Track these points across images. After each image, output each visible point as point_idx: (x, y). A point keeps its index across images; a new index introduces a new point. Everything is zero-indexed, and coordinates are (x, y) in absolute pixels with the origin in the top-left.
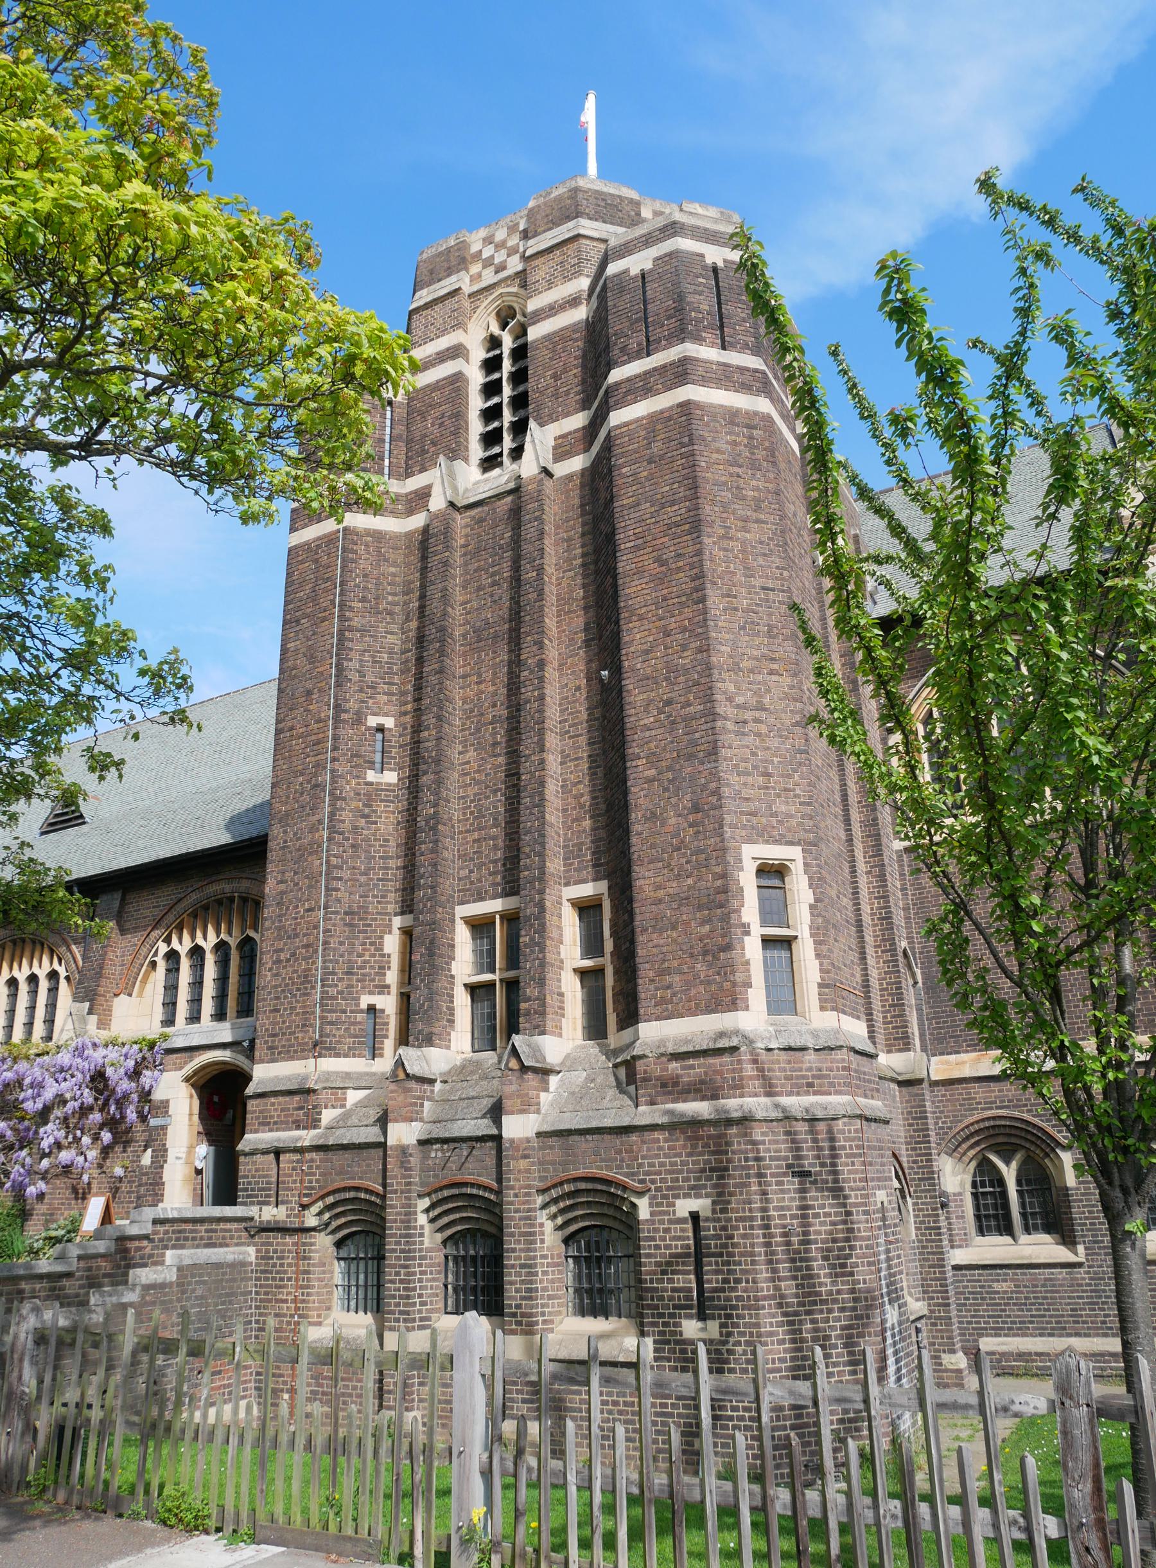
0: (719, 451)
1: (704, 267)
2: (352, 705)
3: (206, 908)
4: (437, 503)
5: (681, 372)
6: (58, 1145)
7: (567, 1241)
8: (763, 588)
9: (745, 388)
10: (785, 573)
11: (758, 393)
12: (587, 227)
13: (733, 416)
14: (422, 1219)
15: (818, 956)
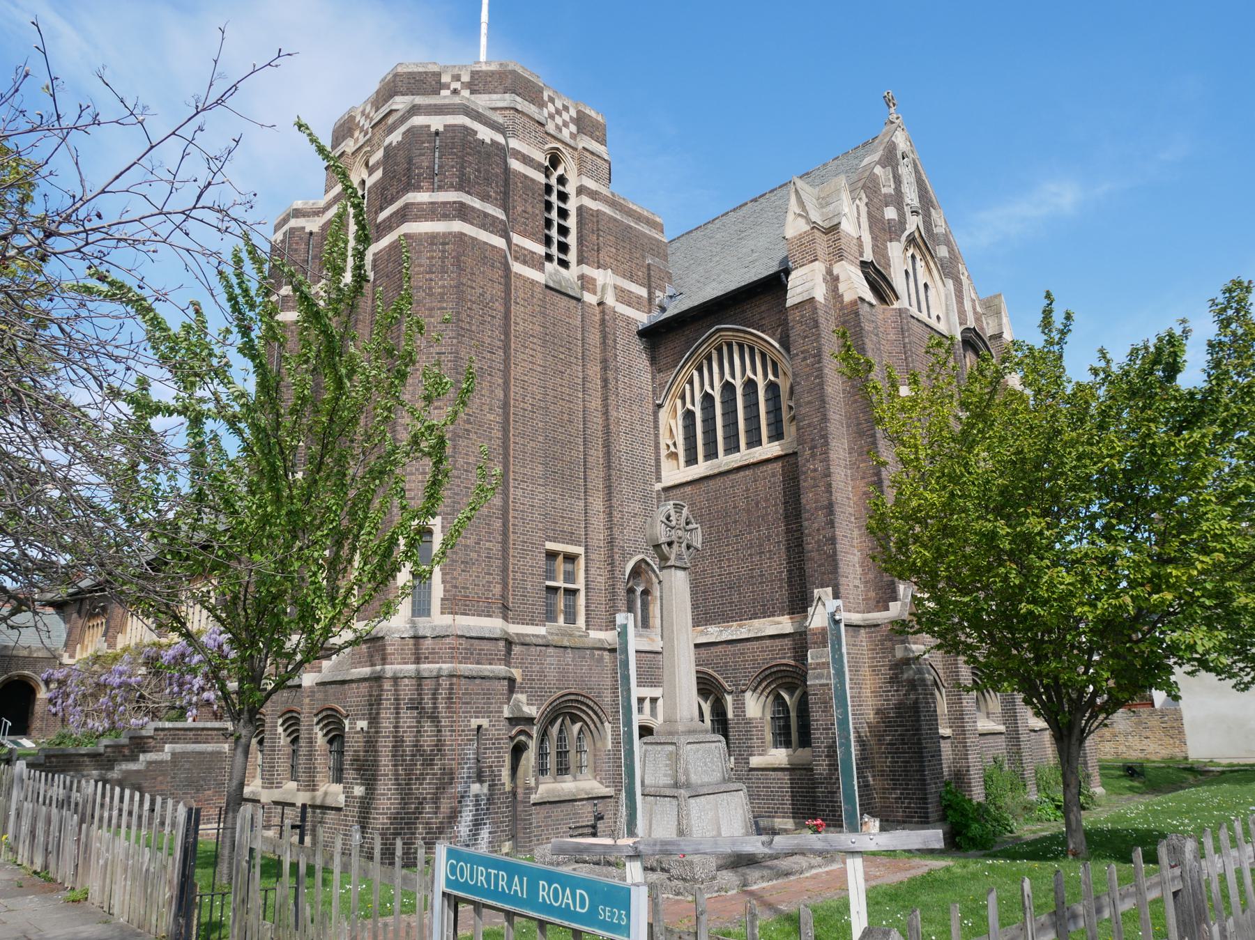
0: (420, 266)
1: (430, 135)
5: (403, 215)
6: (202, 689)
7: (330, 742)
9: (446, 217)
10: (455, 341)
11: (454, 218)
12: (400, 103)
13: (433, 238)
14: (280, 730)
15: (443, 582)
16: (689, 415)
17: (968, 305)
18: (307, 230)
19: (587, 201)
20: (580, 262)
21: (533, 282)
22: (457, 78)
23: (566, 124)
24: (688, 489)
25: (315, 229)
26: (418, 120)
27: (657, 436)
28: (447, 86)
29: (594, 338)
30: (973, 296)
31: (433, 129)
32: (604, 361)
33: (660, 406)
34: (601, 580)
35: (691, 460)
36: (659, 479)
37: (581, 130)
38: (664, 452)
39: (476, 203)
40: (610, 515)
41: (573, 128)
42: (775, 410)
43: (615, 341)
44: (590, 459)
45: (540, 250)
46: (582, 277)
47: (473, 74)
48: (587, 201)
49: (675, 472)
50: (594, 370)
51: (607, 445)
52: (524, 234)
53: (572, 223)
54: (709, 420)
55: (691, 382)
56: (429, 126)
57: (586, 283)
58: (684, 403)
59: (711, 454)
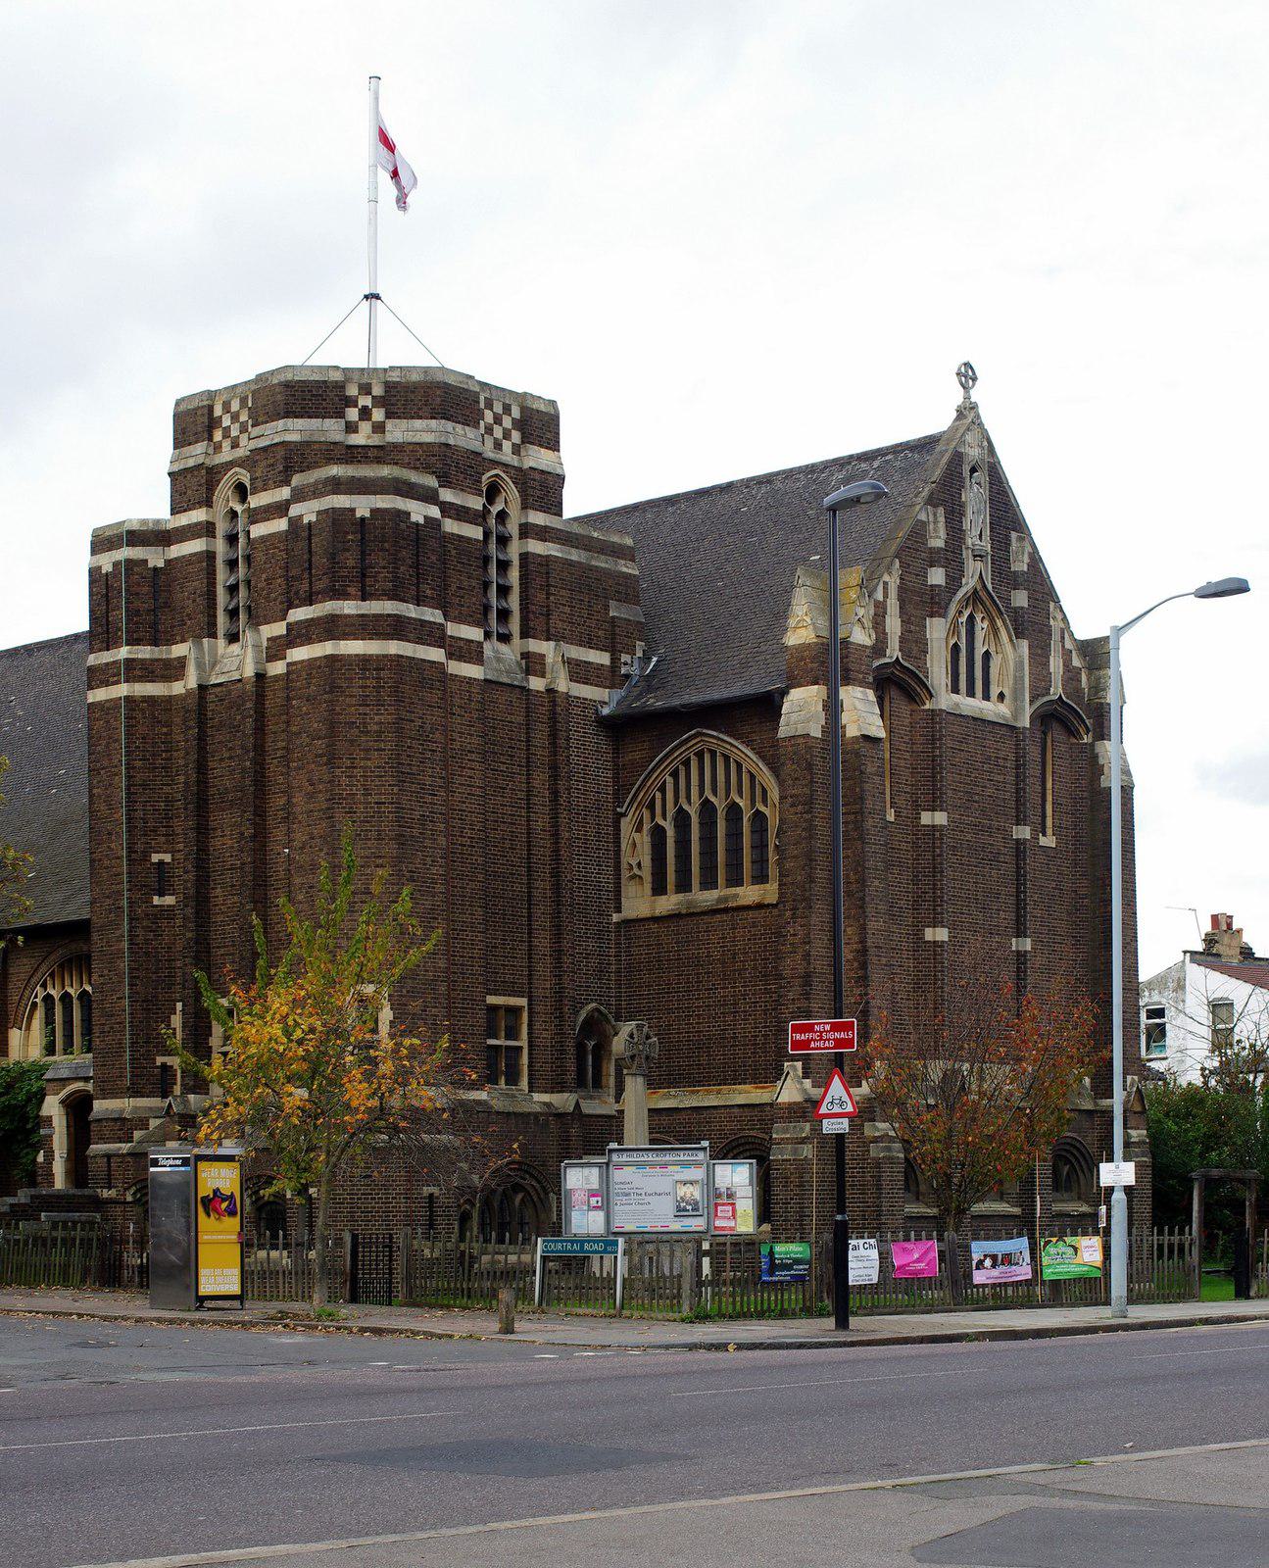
2: (139, 847)
3: (70, 961)
4: (192, 681)
8: (377, 803)
13: (364, 661)
16: (658, 833)
17: (1056, 665)
18: (150, 565)
19: (536, 547)
20: (524, 635)
21: (470, 681)
22: (366, 389)
23: (507, 435)
24: (654, 927)
25: (161, 564)
26: (341, 501)
27: (618, 852)
28: (351, 402)
29: (541, 736)
30: (1069, 645)
31: (358, 515)
32: (554, 767)
33: (624, 815)
34: (545, 1036)
35: (659, 889)
36: (619, 910)
37: (526, 439)
38: (625, 874)
39: (411, 611)
40: (559, 960)
41: (516, 436)
42: (760, 846)
43: (568, 739)
44: (535, 893)
45: (474, 633)
46: (526, 655)
47: (389, 386)
48: (536, 547)
49: (638, 902)
50: (540, 778)
51: (556, 874)
52: (460, 620)
53: (514, 576)
54: (683, 844)
55: (663, 789)
56: (353, 510)
57: (532, 664)
58: (653, 817)
59: (683, 886)
